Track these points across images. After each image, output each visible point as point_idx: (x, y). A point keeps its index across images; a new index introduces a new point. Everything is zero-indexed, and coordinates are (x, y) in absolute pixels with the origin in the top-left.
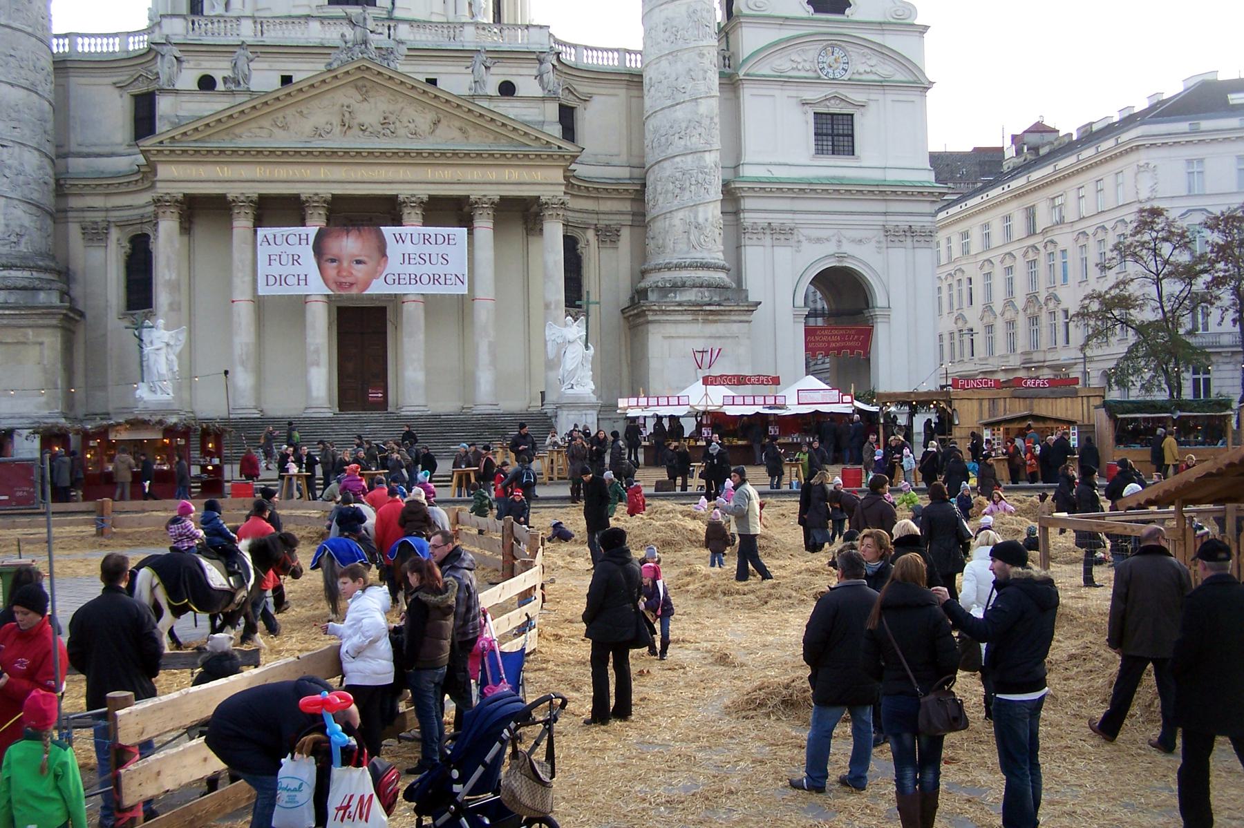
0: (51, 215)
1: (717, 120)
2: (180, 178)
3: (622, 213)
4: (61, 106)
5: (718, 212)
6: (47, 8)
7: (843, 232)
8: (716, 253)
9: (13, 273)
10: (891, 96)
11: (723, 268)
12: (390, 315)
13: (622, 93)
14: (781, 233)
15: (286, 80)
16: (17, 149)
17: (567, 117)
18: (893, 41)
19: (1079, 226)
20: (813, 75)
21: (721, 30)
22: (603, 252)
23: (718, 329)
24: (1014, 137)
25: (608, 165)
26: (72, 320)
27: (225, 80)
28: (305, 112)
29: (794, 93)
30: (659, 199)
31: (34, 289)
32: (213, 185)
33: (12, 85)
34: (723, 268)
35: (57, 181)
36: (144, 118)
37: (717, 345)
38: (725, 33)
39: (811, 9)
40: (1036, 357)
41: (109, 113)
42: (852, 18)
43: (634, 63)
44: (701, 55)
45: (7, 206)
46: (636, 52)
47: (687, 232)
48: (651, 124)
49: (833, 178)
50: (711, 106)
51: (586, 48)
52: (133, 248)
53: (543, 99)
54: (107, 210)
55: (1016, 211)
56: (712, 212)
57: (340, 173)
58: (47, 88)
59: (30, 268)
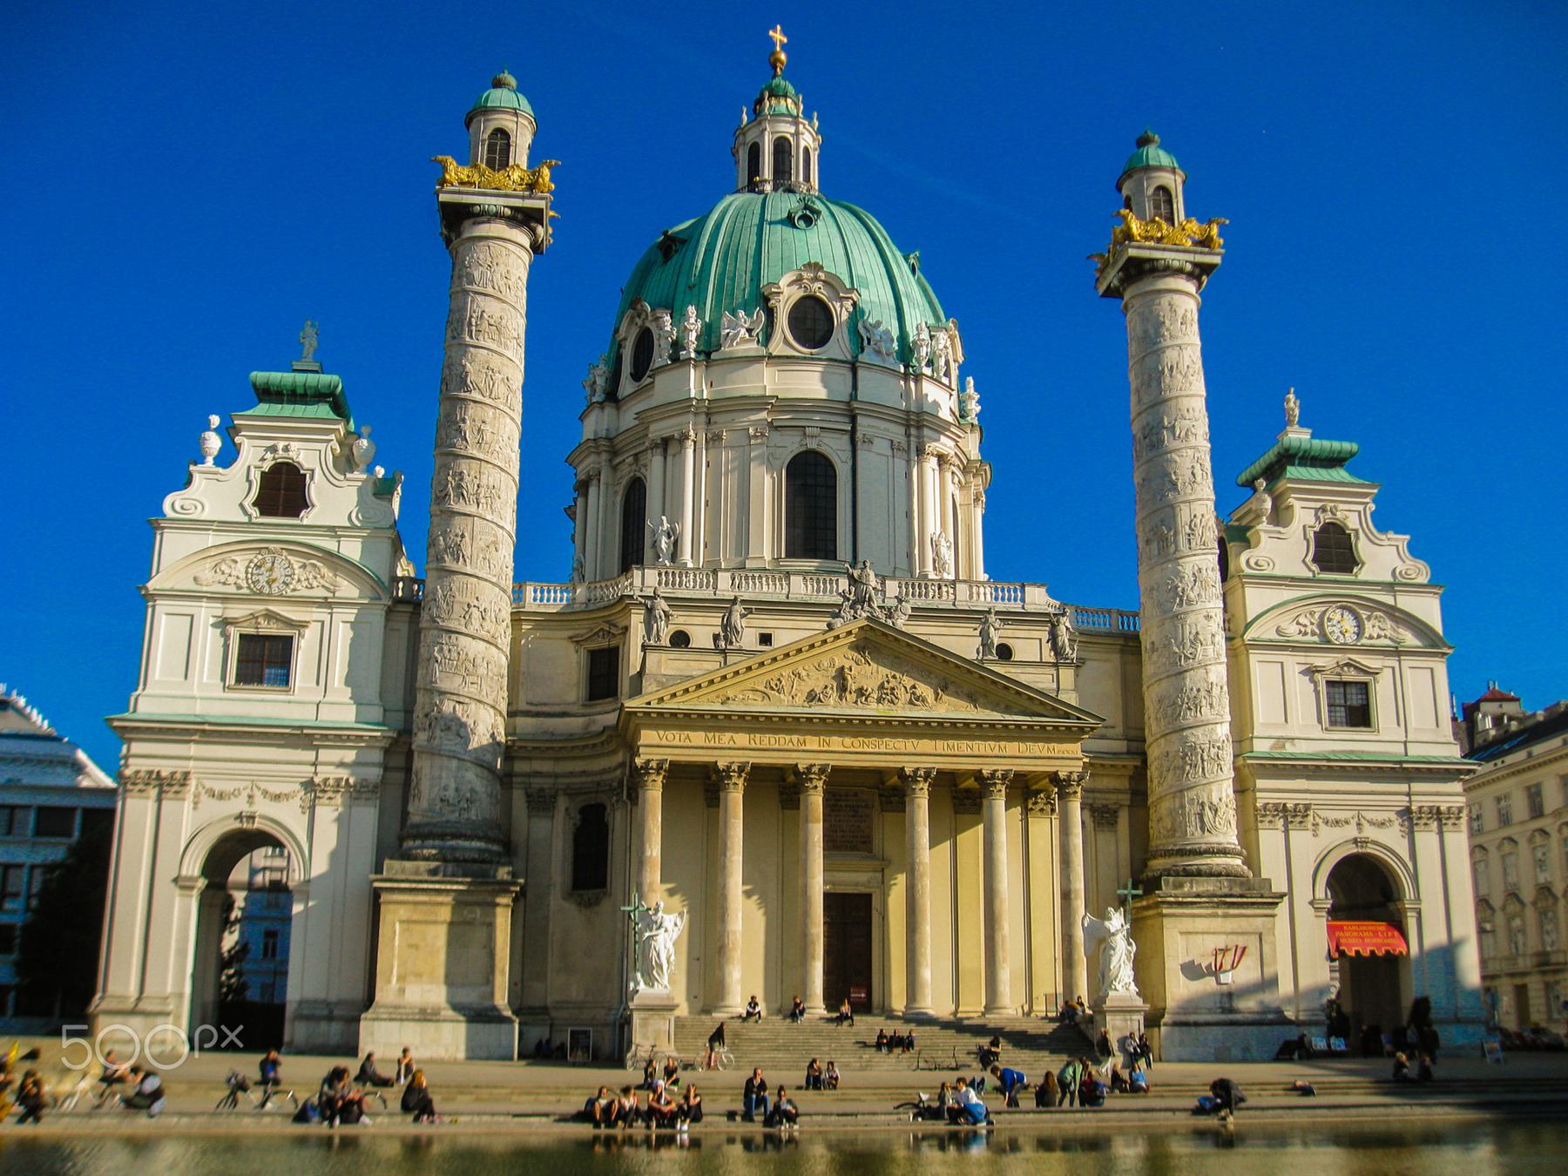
3: (1118, 791)
5: (1231, 791)
9: (462, 843)
10: (1407, 662)
12: (875, 903)
13: (1116, 658)
15: (766, 639)
16: (473, 705)
18: (1406, 602)
22: (1100, 836)
25: (1103, 737)
27: (716, 637)
28: (804, 673)
31: (483, 861)
32: (702, 752)
33: (474, 638)
34: (1240, 854)
37: (1241, 941)
39: (1315, 567)
41: (566, 669)
42: (1361, 577)
44: (1208, 617)
45: (459, 769)
49: (1352, 752)
50: (1218, 673)
54: (556, 776)
57: (836, 743)
59: (479, 839)
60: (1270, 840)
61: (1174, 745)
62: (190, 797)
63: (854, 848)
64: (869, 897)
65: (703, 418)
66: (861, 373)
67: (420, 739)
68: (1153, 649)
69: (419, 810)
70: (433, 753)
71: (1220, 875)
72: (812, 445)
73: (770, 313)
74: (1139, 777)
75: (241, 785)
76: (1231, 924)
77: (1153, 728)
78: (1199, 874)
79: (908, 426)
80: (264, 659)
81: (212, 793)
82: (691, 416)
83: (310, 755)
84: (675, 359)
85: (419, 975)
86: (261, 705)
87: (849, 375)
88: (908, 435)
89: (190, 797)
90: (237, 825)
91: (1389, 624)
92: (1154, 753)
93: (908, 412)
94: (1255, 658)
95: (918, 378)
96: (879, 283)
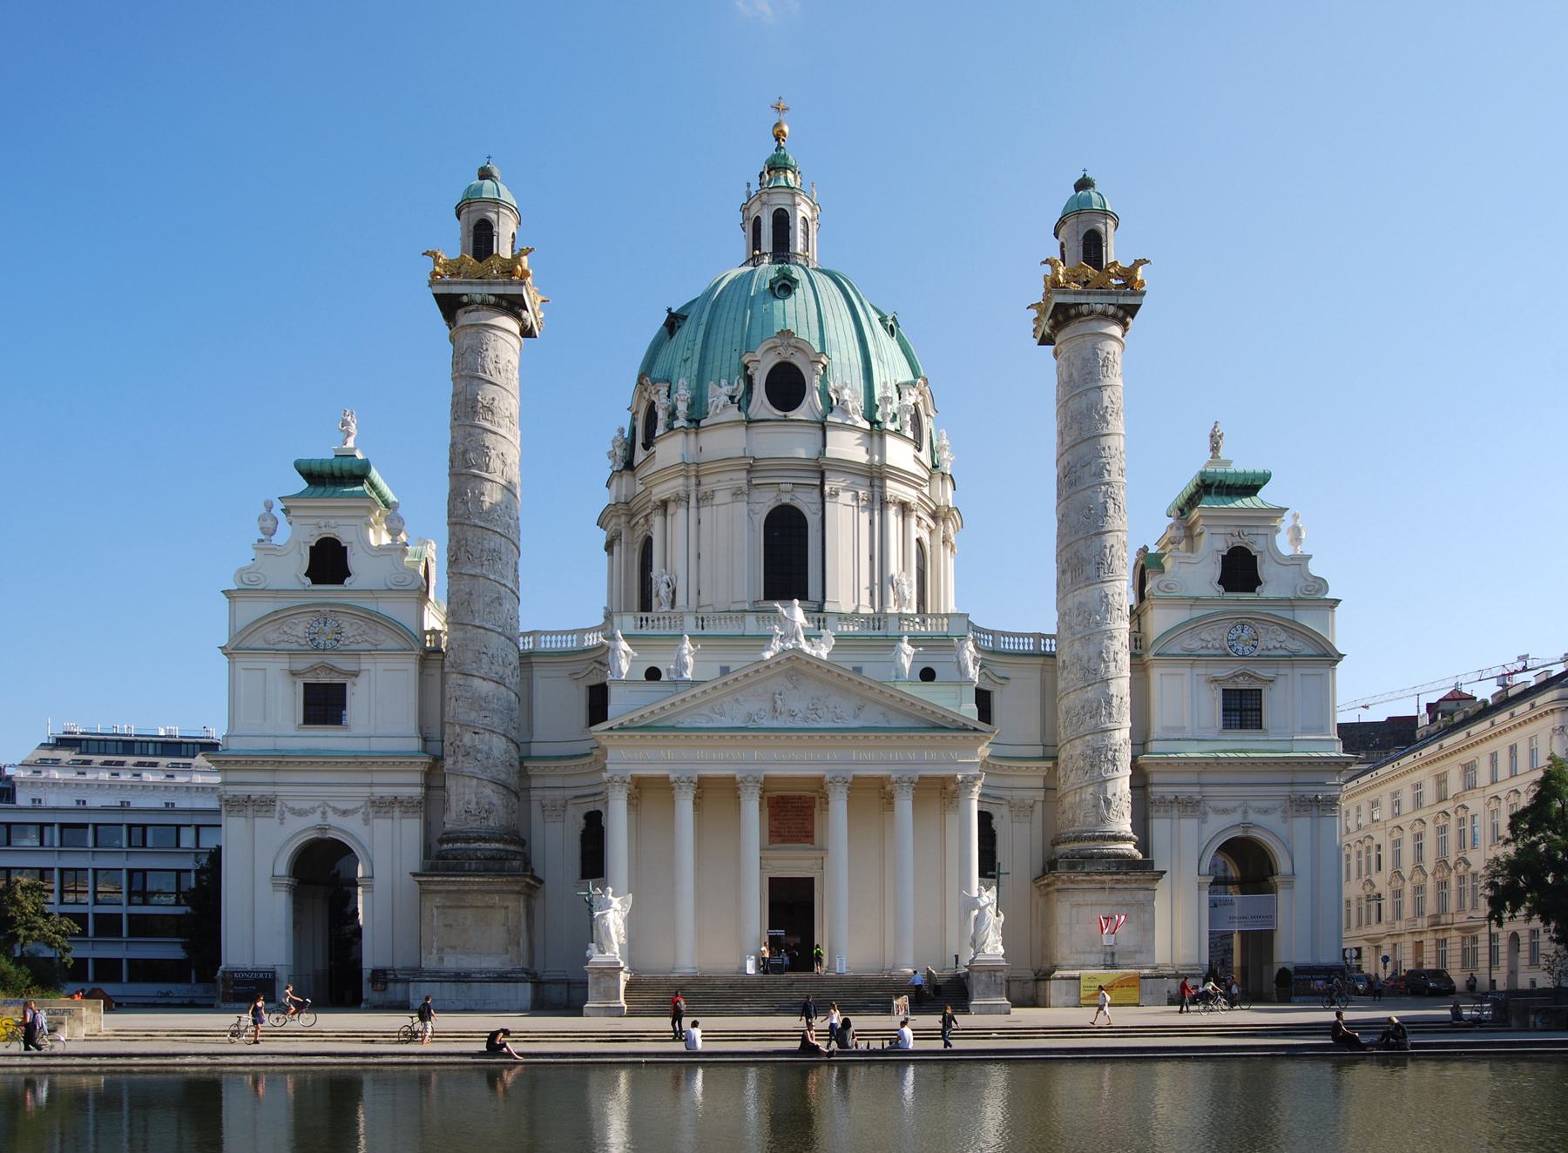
0: (516, 794)
1: (1127, 699)
2: (628, 759)
4: (526, 698)
6: (516, 610)
7: (1254, 804)
8: (1124, 825)
9: (483, 845)
10: (1298, 671)
11: (1130, 839)
14: (1190, 806)
15: (725, 671)
17: (983, 699)
19: (1492, 790)
20: (1220, 652)
21: (1132, 612)
23: (1127, 896)
24: (1429, 706)
26: (532, 886)
29: (1202, 671)
30: (1070, 779)
34: (1130, 839)
35: (521, 763)
36: (598, 704)
38: (1136, 615)
40: (1443, 920)
43: (1048, 646)
46: (1051, 637)
47: (1096, 806)
48: (1063, 705)
50: (1121, 686)
51: (1004, 634)
52: (587, 824)
53: (959, 684)
55: (1426, 776)
56: (1121, 785)
58: (513, 680)
59: (497, 841)
60: (1160, 827)
61: (1078, 747)
62: (277, 815)
63: (799, 841)
64: (812, 879)
65: (693, 481)
66: (829, 434)
67: (449, 762)
68: (1064, 667)
69: (452, 820)
70: (459, 774)
71: (1108, 856)
72: (786, 500)
73: (749, 381)
74: (1052, 774)
75: (316, 804)
76: (1117, 897)
77: (1063, 734)
78: (1092, 857)
79: (872, 479)
80: (324, 704)
81: (293, 811)
82: (681, 481)
83: (367, 778)
84: (670, 428)
85: (454, 948)
86: (324, 738)
87: (820, 433)
88: (872, 486)
89: (277, 815)
90: (313, 835)
91: (1283, 637)
92: (1063, 756)
93: (870, 466)
94: (1155, 674)
95: (882, 433)
96: (851, 345)
